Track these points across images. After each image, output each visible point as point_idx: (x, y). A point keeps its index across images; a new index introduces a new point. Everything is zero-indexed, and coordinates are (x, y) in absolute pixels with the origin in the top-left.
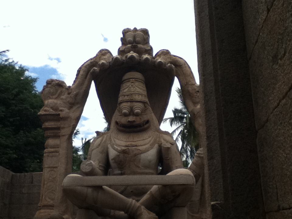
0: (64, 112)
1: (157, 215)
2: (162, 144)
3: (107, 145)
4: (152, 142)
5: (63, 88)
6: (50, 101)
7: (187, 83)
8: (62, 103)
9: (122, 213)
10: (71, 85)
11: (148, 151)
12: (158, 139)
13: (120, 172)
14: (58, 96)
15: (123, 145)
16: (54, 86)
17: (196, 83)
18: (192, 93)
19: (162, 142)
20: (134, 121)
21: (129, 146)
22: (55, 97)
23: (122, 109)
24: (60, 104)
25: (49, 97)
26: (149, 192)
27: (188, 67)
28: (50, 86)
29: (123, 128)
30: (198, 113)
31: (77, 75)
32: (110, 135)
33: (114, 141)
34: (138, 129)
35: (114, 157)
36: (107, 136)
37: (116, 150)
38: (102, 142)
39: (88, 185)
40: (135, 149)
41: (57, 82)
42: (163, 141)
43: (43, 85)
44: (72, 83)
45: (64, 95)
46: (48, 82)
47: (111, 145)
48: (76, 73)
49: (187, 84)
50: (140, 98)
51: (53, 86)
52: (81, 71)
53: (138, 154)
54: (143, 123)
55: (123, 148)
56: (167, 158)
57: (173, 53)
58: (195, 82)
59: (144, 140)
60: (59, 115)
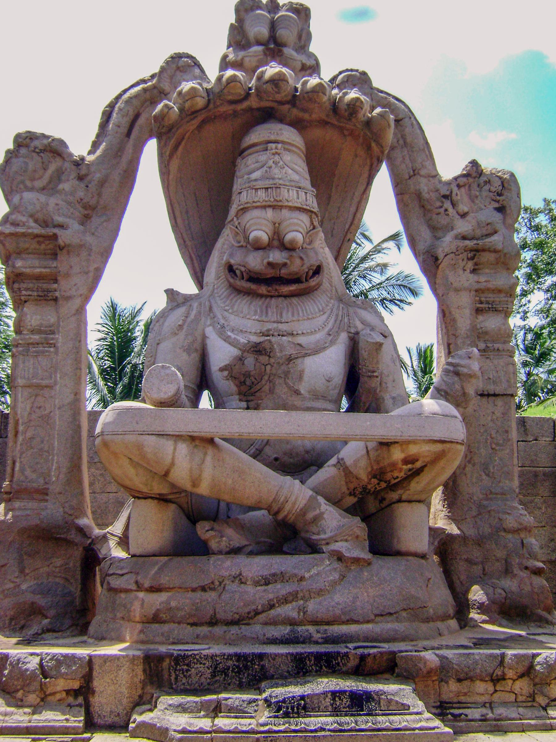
0: (70, 230)
1: (363, 520)
2: (357, 333)
3: (204, 331)
4: (330, 325)
5: (64, 159)
6: (28, 196)
7: (415, 173)
8: (61, 202)
9: (263, 512)
10: (85, 154)
11: (325, 348)
12: (346, 320)
13: (244, 404)
14: (50, 182)
15: (253, 331)
16: (37, 153)
17: (438, 174)
18: (428, 201)
19: (356, 327)
20: (285, 265)
21: (271, 332)
22: (41, 186)
23: (248, 230)
24: (57, 208)
25: (23, 182)
26: (333, 461)
27: (416, 127)
28: (23, 151)
29: (248, 283)
30: (446, 256)
31: (103, 126)
32: (207, 304)
33: (224, 318)
34: (293, 288)
35: (227, 362)
36: (200, 304)
37: (233, 343)
38: (189, 319)
39: (177, 433)
40: (289, 341)
41: (45, 142)
42: (360, 326)
43: (6, 149)
44: (89, 148)
45: (68, 180)
46: (20, 140)
47: (214, 327)
48: (97, 119)
49: (415, 175)
50: (300, 200)
51: (34, 151)
52: (114, 115)
53: (297, 358)
54: (307, 273)
55: (255, 339)
56: (374, 372)
57: (375, 84)
58: (436, 170)
59: (308, 319)
60: (55, 237)
